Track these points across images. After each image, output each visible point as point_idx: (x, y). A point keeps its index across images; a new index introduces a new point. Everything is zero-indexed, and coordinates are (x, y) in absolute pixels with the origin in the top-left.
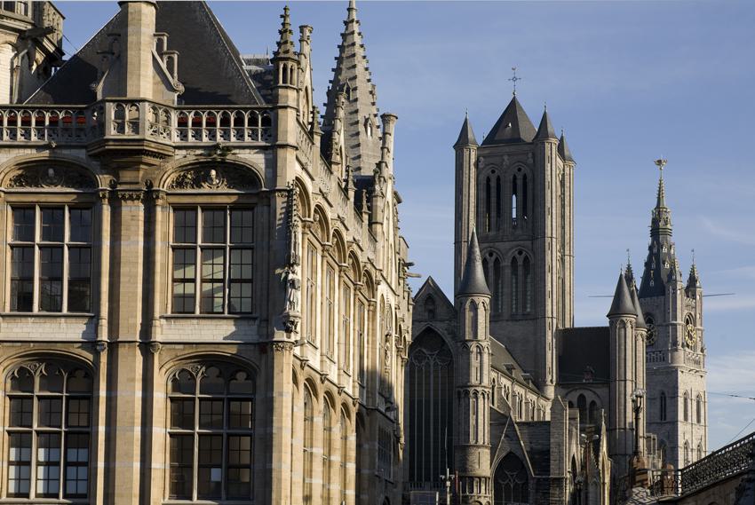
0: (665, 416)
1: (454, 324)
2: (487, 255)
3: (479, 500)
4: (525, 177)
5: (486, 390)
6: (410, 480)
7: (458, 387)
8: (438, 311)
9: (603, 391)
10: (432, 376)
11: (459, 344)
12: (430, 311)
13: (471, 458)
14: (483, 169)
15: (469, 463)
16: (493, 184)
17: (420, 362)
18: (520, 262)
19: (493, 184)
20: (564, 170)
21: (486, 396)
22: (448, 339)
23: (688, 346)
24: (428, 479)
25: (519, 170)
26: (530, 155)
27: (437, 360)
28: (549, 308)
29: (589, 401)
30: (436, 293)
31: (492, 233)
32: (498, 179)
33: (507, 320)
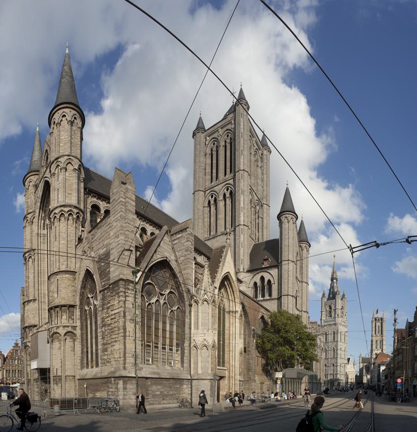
3: (58, 331)
9: (274, 272)
16: (214, 153)
28: (242, 218)
31: (213, 183)
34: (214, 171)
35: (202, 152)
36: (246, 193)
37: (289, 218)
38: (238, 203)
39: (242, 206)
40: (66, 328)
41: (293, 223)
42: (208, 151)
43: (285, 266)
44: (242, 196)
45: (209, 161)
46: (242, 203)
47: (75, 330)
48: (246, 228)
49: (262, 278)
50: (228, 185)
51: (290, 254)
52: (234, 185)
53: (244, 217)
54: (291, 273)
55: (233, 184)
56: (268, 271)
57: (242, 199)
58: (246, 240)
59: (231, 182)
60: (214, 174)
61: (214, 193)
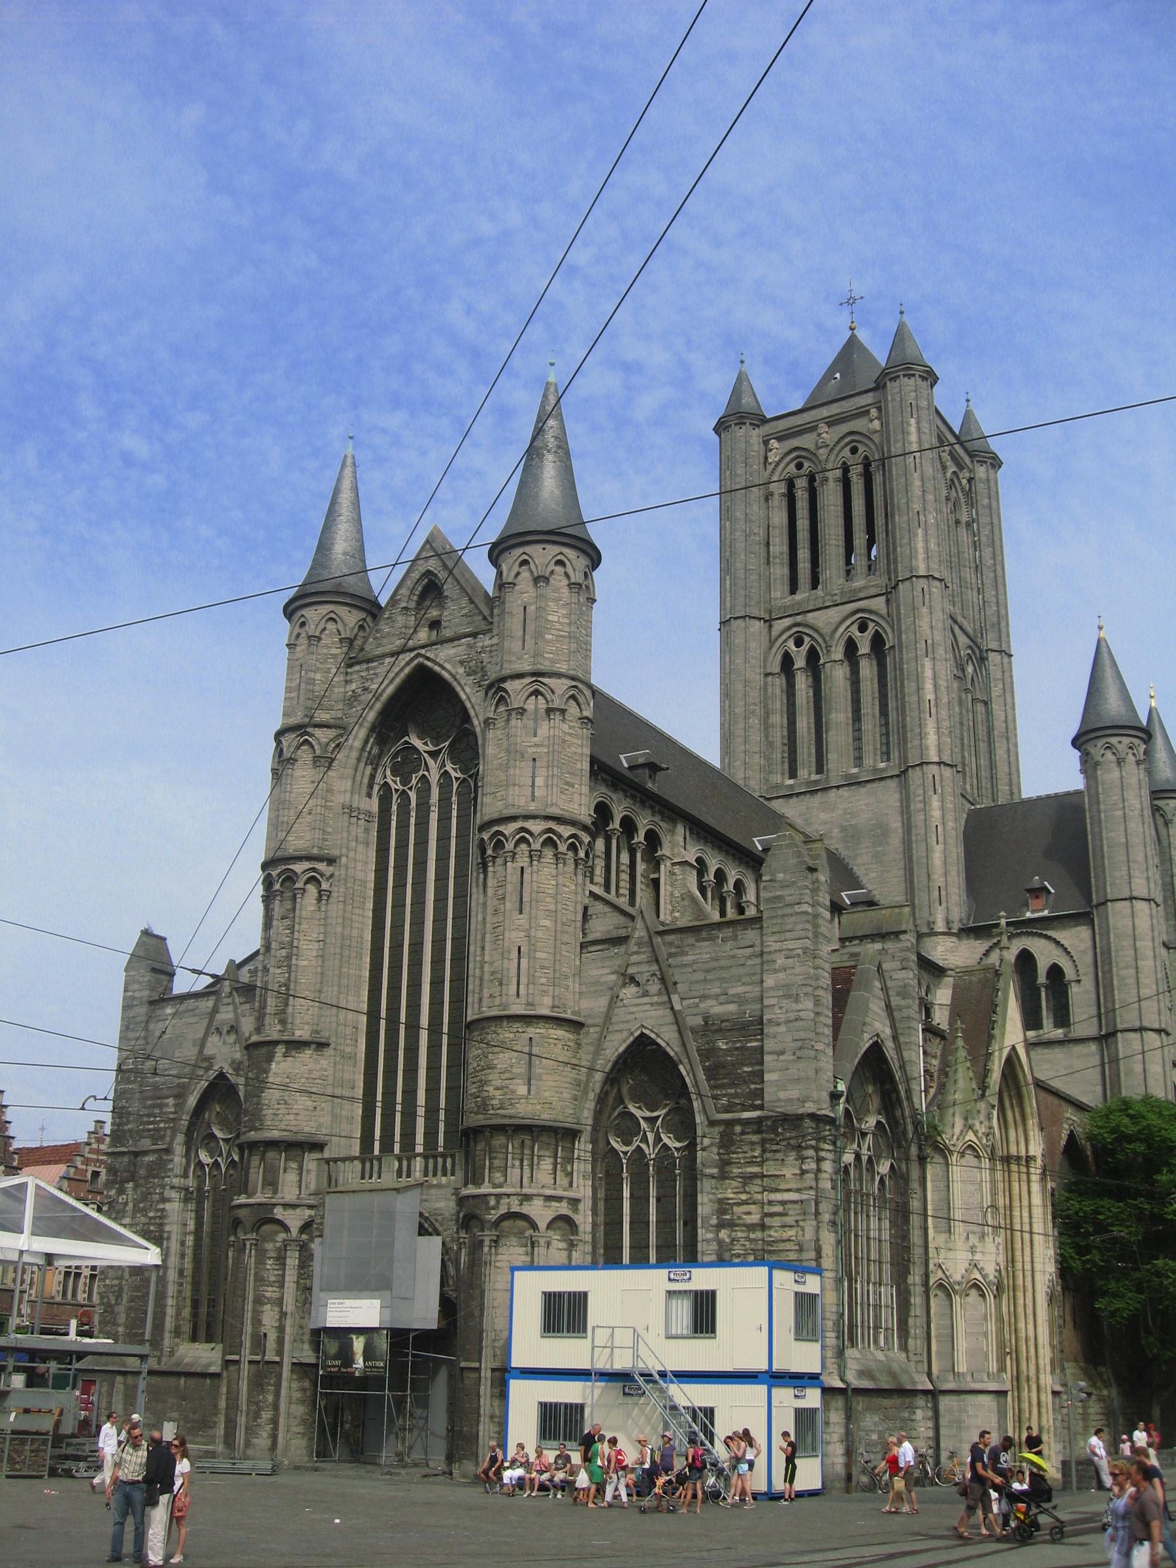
1: (485, 641)
2: (791, 645)
3: (526, 1209)
4: (867, 463)
5: (566, 831)
7: (483, 828)
9: (1076, 938)
10: (434, 817)
14: (778, 464)
15: (495, 1078)
17: (405, 781)
18: (864, 648)
19: (802, 496)
21: (562, 848)
22: (469, 693)
24: (387, 1147)
26: (874, 412)
27: (449, 767)
28: (931, 739)
29: (1043, 966)
31: (798, 597)
32: (812, 478)
33: (838, 787)
34: (803, 554)
38: (913, 685)
39: (929, 695)
40: (554, 1204)
41: (1138, 763)
43: (1118, 915)
45: (779, 517)
46: (929, 686)
47: (576, 1210)
48: (947, 772)
49: (1026, 960)
51: (1136, 873)
52: (893, 617)
54: (1145, 945)
55: (884, 612)
56: (1049, 933)
57: (928, 673)
58: (950, 816)
59: (879, 604)
60: (804, 566)
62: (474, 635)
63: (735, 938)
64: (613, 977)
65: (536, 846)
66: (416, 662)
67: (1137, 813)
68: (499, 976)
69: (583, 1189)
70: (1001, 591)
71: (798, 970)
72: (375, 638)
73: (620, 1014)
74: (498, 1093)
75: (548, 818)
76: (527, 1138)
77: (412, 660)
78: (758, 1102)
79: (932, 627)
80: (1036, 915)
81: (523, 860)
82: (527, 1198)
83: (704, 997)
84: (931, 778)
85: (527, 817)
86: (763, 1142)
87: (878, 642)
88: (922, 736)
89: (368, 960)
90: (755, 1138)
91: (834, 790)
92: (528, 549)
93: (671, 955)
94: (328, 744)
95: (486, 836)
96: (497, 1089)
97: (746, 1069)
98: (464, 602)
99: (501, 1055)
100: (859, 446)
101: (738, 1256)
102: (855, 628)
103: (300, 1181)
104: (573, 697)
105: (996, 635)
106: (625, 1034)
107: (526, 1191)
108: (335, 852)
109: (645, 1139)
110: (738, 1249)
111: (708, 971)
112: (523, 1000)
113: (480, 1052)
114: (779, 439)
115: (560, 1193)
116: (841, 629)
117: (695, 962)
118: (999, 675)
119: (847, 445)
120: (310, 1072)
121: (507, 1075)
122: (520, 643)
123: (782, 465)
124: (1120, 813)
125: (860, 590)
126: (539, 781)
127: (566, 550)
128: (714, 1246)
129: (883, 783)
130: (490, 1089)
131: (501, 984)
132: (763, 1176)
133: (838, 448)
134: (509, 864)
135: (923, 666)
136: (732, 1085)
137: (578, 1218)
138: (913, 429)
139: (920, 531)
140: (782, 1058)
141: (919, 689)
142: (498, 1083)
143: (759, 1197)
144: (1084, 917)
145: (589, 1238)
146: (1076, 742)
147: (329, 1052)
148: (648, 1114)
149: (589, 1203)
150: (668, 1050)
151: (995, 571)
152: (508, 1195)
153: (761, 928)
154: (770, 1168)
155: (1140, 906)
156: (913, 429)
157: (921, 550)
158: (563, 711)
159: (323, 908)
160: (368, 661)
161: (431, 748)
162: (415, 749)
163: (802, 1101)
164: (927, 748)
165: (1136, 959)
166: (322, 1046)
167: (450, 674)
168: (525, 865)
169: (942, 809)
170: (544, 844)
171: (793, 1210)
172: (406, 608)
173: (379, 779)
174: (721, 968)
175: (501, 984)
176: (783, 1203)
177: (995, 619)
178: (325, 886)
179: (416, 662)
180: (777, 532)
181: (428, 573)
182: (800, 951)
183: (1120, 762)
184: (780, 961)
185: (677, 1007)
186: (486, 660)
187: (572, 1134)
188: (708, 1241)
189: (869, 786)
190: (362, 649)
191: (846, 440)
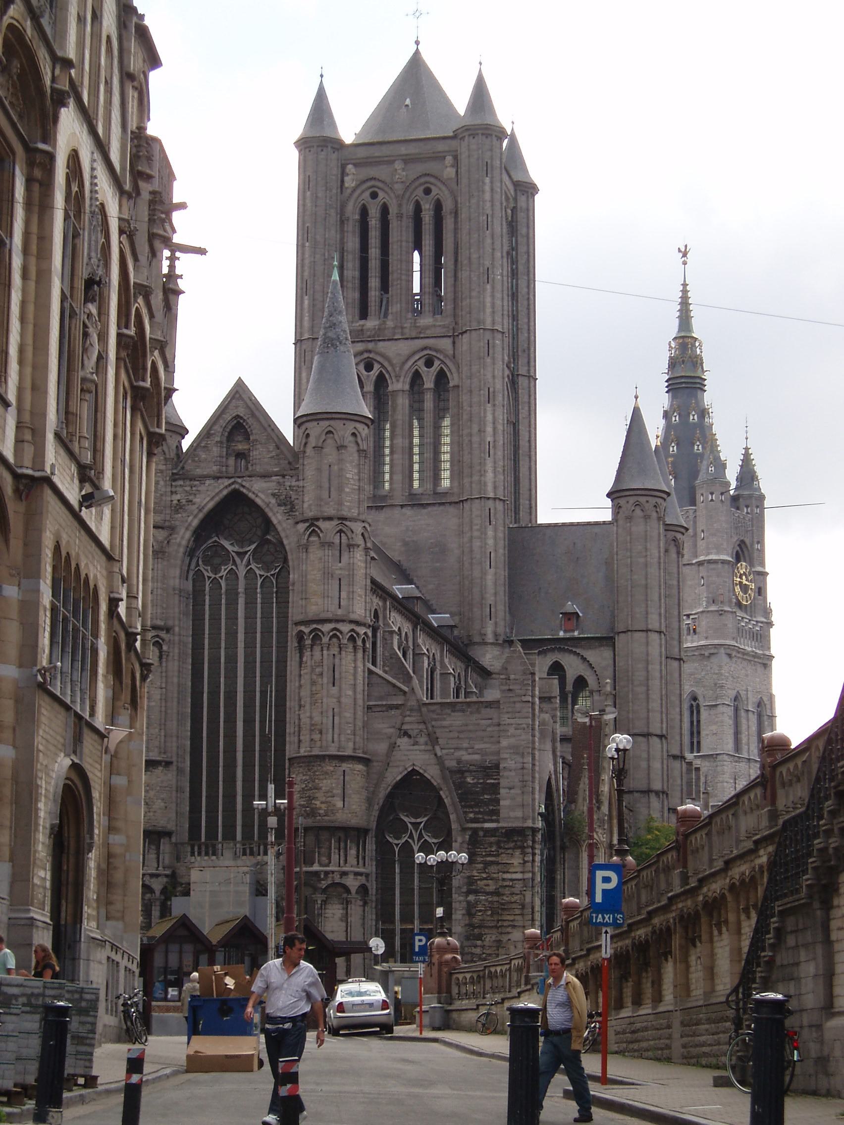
0: (699, 743)
1: (290, 482)
3: (344, 881)
4: (438, 207)
5: (362, 630)
6: (191, 839)
8: (254, 454)
9: (599, 657)
11: (302, 527)
12: (241, 455)
13: (325, 784)
14: (354, 190)
15: (320, 795)
16: (374, 222)
17: (216, 570)
19: (374, 222)
20: (515, 199)
21: (360, 643)
22: (277, 517)
23: (739, 604)
24: (229, 835)
25: (428, 191)
26: (449, 159)
28: (490, 475)
29: (571, 676)
30: (253, 415)
31: (371, 323)
32: (385, 210)
33: (402, 506)
34: (374, 282)
35: (333, 212)
36: (499, 398)
37: (649, 507)
39: (489, 439)
40: (359, 877)
41: (659, 519)
42: (352, 213)
44: (489, 407)
45: (353, 243)
46: (489, 429)
48: (500, 506)
49: (557, 669)
50: (434, 353)
53: (495, 472)
57: (489, 417)
61: (379, 358)
62: (284, 476)
63: (479, 713)
64: (392, 730)
65: (345, 641)
66: (233, 486)
67: (656, 560)
68: (318, 727)
69: (371, 868)
70: (532, 319)
71: (523, 737)
72: (193, 461)
73: (397, 755)
74: (323, 806)
75: (351, 622)
76: (342, 835)
77: (230, 485)
78: (494, 818)
79: (494, 377)
80: (568, 635)
81: (335, 650)
82: (344, 874)
83: (457, 749)
84: (488, 511)
85: (337, 621)
86: (498, 844)
87: (441, 378)
88: (483, 472)
89: (190, 700)
90: (493, 839)
91: (399, 508)
92: (332, 423)
93: (436, 720)
94: (162, 542)
95: (306, 630)
96: (322, 803)
97: (486, 796)
98: (272, 447)
99: (325, 781)
100: (433, 187)
101: (480, 911)
102: (421, 363)
103: (158, 858)
104: (362, 534)
105: (526, 360)
106: (401, 769)
107: (345, 869)
108: (170, 623)
109: (411, 836)
110: (480, 907)
111: (459, 732)
112: (336, 744)
113: (308, 778)
114: (355, 165)
115: (361, 870)
116: (410, 363)
117: (451, 726)
118: (526, 399)
119: (421, 184)
120: (162, 782)
121: (330, 794)
122: (327, 492)
123: (358, 191)
124: (642, 560)
125: (427, 328)
126: (344, 595)
127: (358, 425)
128: (464, 904)
129: (442, 508)
130: (318, 803)
131: (321, 733)
132: (498, 863)
133: (413, 187)
134: (325, 652)
135: (485, 410)
136: (476, 805)
137: (368, 885)
138: (487, 188)
139: (488, 287)
140: (512, 791)
141: (481, 431)
142: (324, 799)
143: (495, 875)
144: (608, 641)
145: (374, 898)
146: (608, 495)
147: (174, 767)
148: (413, 820)
149: (374, 876)
150: (432, 781)
151: (528, 299)
152: (333, 872)
153: (499, 708)
154: (504, 859)
155: (654, 637)
156: (487, 188)
157: (488, 305)
158: (358, 546)
159: (164, 664)
160: (191, 480)
161: (236, 549)
162: (223, 547)
163: (524, 819)
164: (485, 484)
165: (648, 680)
166: (168, 764)
167: (263, 501)
168: (336, 653)
169: (495, 538)
170: (348, 640)
171: (519, 886)
172: (221, 442)
173: (193, 567)
174: (470, 731)
175: (321, 733)
176: (512, 880)
177: (526, 345)
178: (165, 648)
179: (233, 486)
180: (350, 257)
181: (238, 416)
182: (524, 726)
183: (647, 517)
184: (512, 731)
185: (439, 754)
186: (293, 497)
187: (366, 831)
188: (460, 902)
189: (430, 509)
190: (183, 468)
191: (422, 180)
